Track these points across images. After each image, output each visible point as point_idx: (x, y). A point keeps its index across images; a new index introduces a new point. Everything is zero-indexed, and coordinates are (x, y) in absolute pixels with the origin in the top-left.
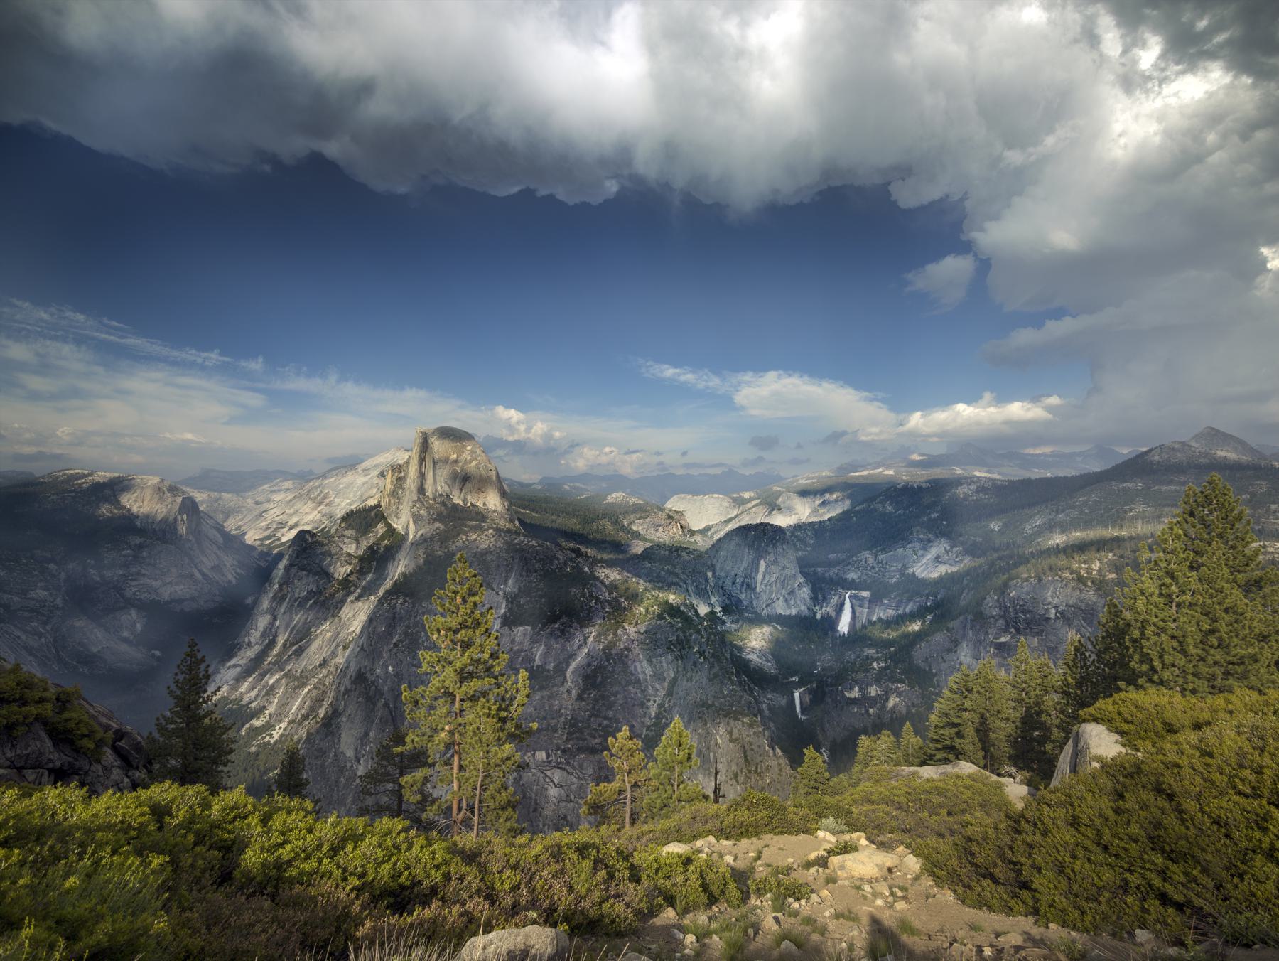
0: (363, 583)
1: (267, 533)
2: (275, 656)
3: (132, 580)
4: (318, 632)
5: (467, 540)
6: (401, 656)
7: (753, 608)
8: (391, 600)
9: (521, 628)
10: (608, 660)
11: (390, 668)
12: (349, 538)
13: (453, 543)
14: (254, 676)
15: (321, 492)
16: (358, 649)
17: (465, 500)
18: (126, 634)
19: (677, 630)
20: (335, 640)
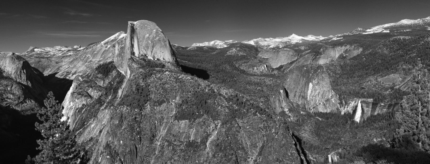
4: (88, 124)
5: (156, 77)
7: (305, 109)
9: (183, 121)
10: (228, 137)
11: (121, 142)
12: (100, 78)
13: (149, 79)
16: (106, 133)
17: (154, 57)
19: (264, 121)
20: (95, 128)
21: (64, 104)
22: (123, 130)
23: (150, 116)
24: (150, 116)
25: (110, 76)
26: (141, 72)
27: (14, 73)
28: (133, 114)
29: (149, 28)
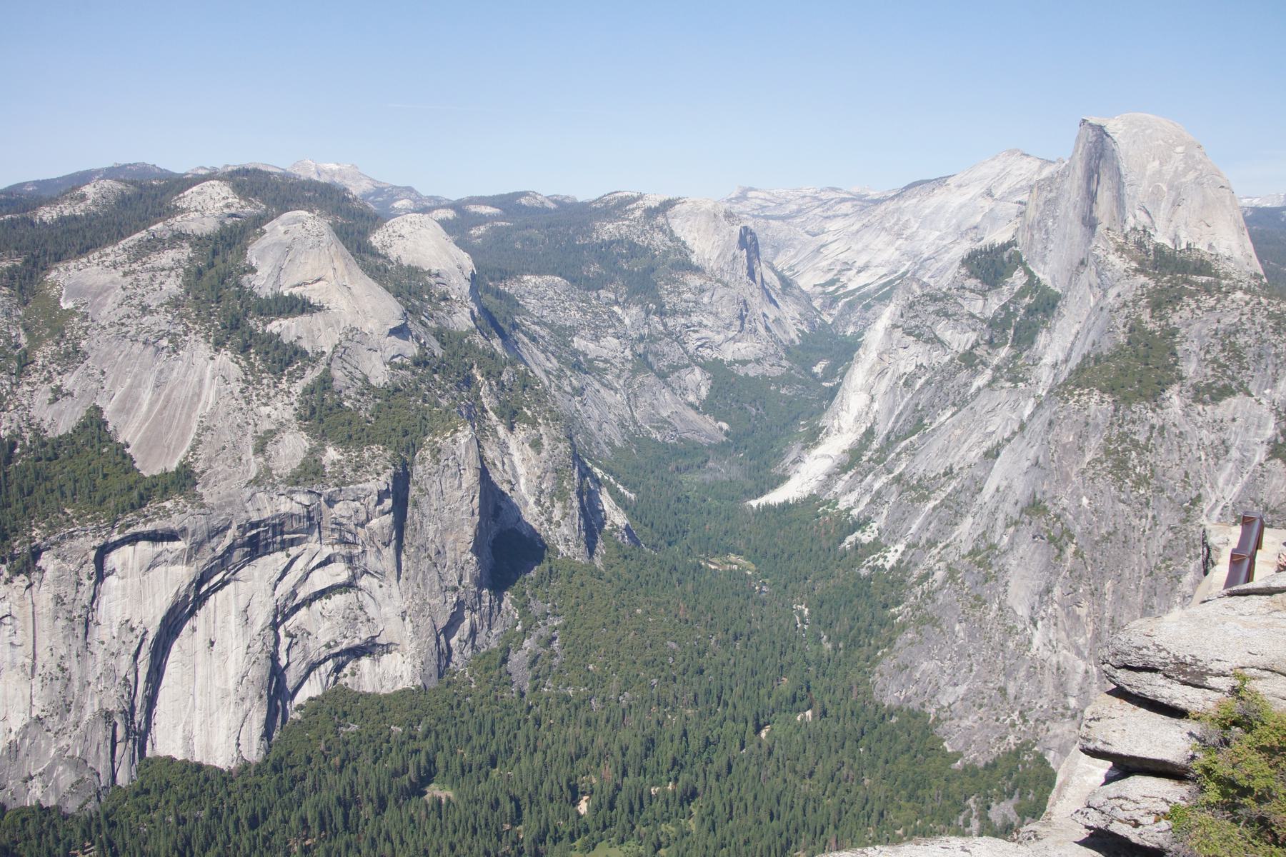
0: (996, 361)
1: (830, 276)
2: (877, 451)
3: (694, 331)
4: (934, 426)
6: (1100, 484)
8: (1080, 395)
11: (1085, 501)
12: (972, 291)
13: (1174, 310)
14: (850, 473)
15: (899, 219)
16: (1028, 464)
17: (1175, 239)
18: (691, 398)
20: (965, 441)
21: (863, 356)
22: (1089, 463)
23: (1181, 433)
24: (1181, 433)
25: (1005, 288)
26: (1142, 286)
27: (718, 257)
28: (1124, 419)
29: (1161, 142)
